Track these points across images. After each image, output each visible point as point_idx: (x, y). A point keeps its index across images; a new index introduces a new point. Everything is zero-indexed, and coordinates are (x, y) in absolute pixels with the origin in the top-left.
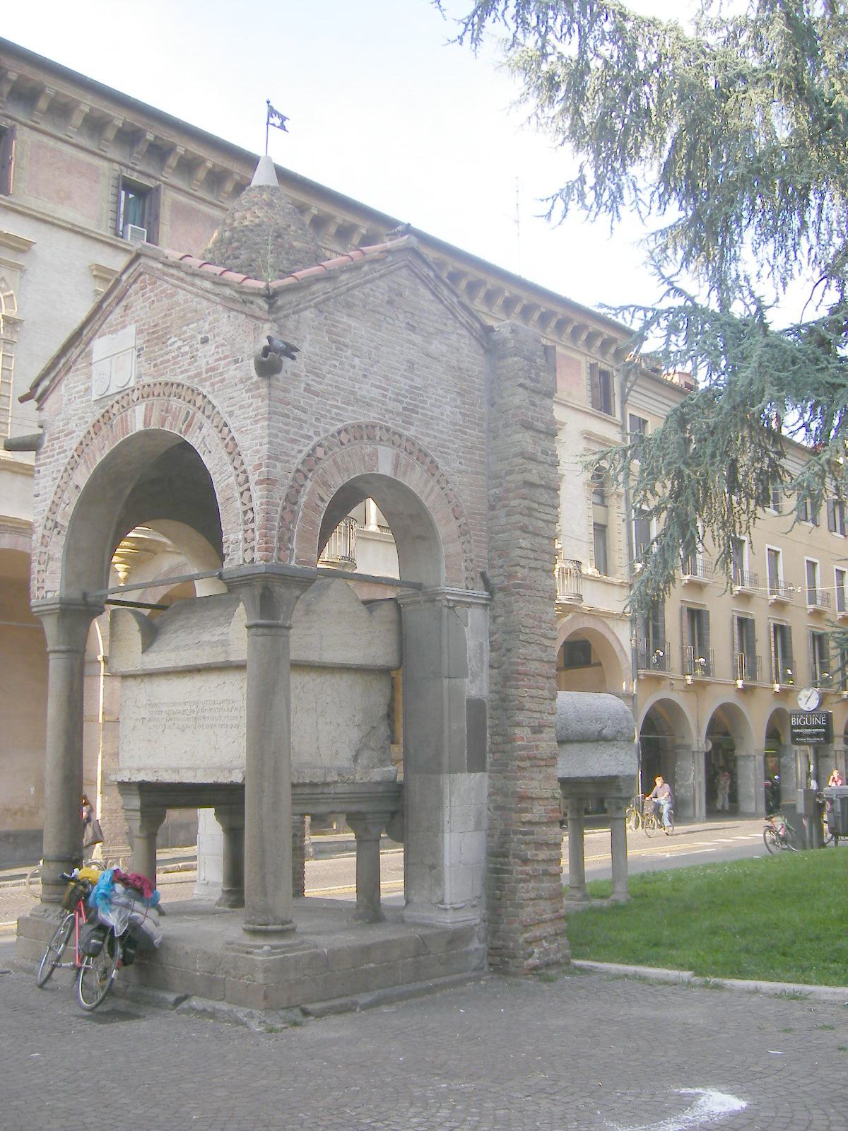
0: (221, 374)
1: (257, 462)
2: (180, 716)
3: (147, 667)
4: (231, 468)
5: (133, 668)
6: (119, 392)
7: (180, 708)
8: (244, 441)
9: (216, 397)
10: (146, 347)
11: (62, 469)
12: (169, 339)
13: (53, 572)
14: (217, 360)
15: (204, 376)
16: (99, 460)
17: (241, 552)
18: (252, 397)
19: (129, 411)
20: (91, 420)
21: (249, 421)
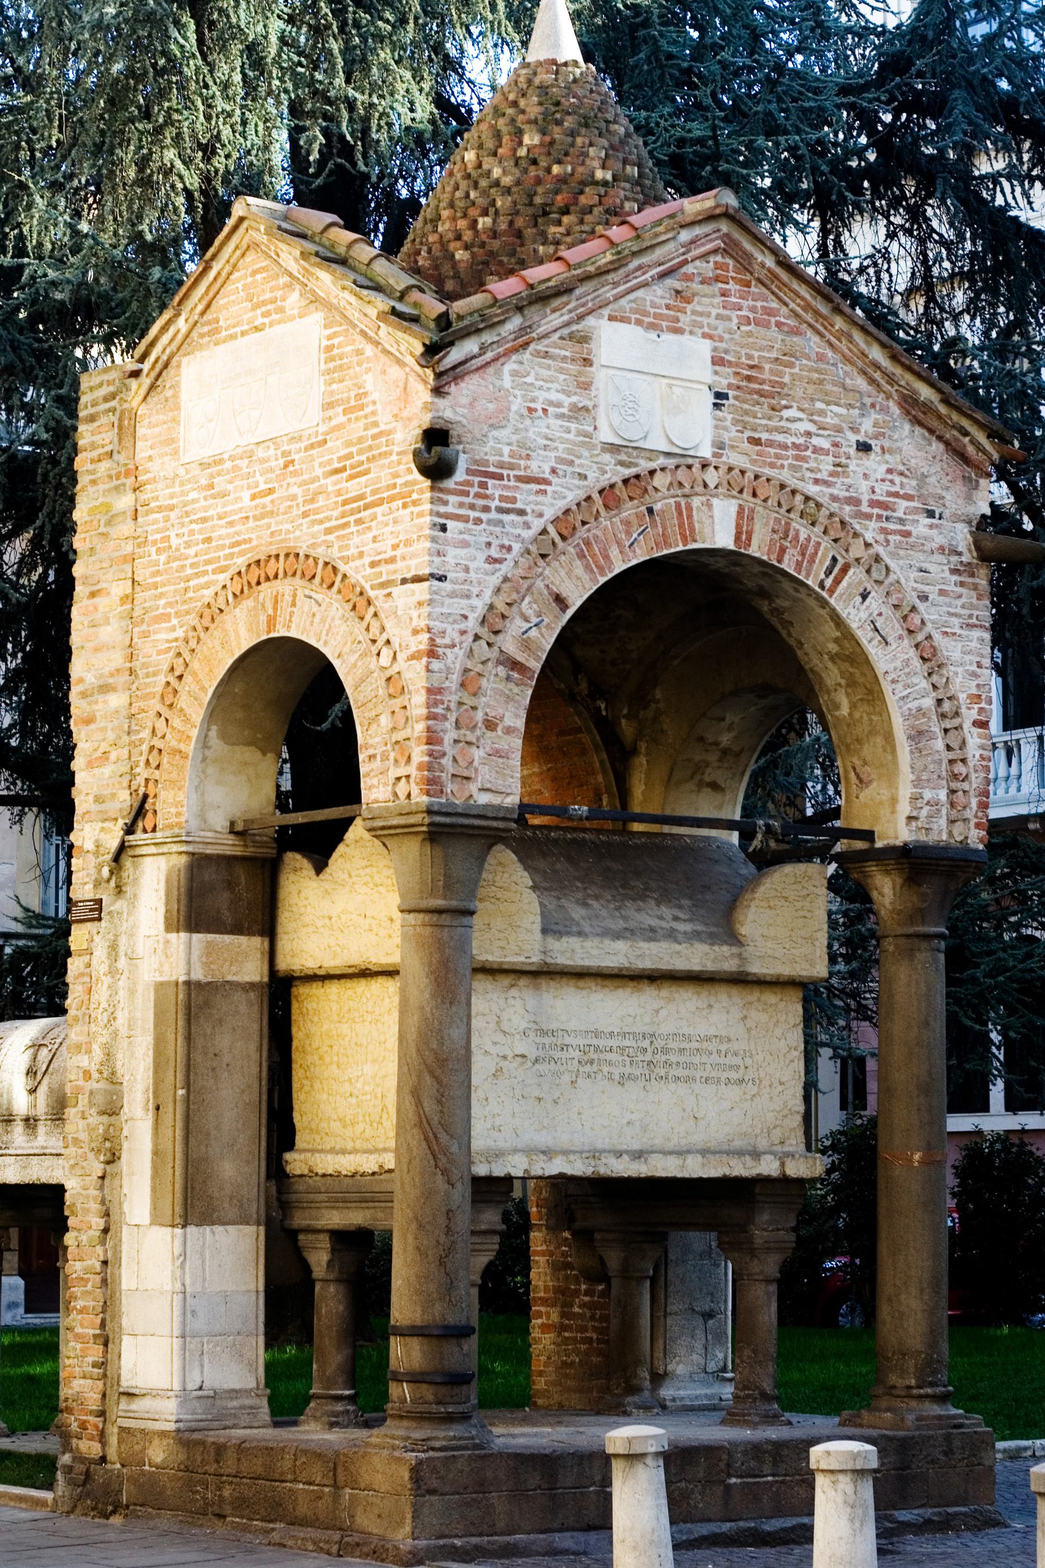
0: (901, 521)
1: (974, 691)
2: (613, 1057)
3: (559, 961)
4: (924, 684)
5: (522, 959)
6: (668, 454)
7: (613, 1043)
8: (950, 649)
9: (892, 555)
10: (736, 398)
11: (517, 547)
12: (786, 407)
13: (497, 753)
14: (890, 494)
15: (865, 508)
16: (619, 567)
17: (943, 822)
18: (962, 584)
19: (696, 502)
20: (596, 479)
21: (956, 621)
